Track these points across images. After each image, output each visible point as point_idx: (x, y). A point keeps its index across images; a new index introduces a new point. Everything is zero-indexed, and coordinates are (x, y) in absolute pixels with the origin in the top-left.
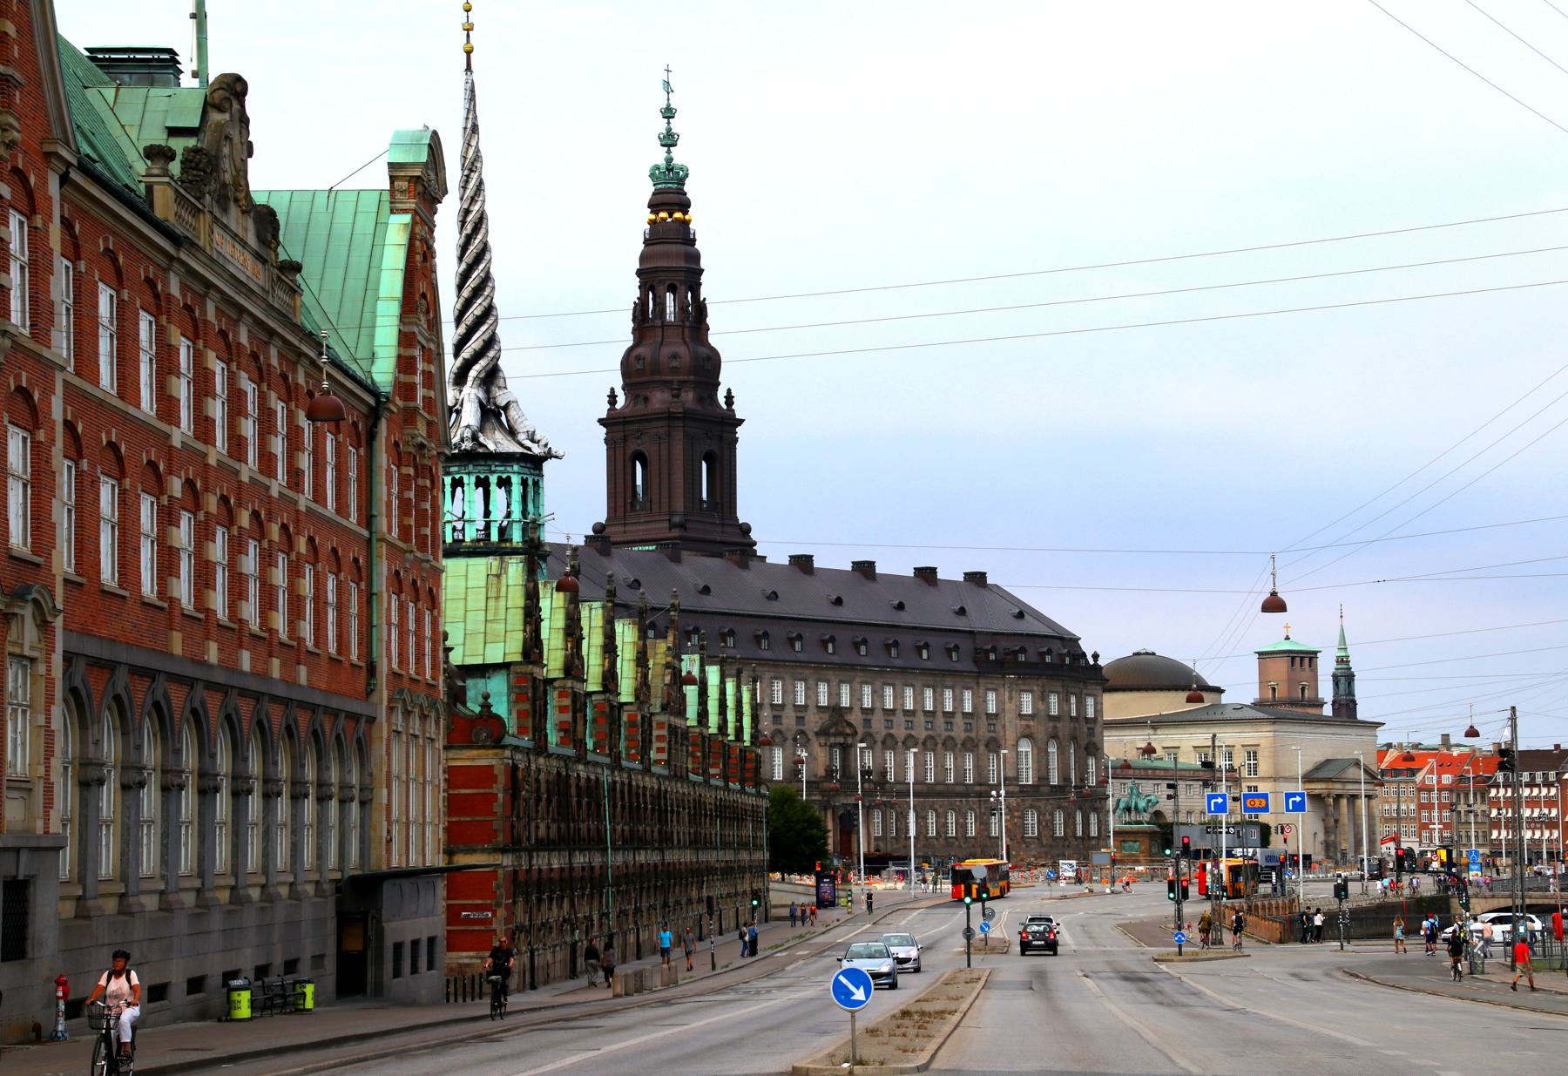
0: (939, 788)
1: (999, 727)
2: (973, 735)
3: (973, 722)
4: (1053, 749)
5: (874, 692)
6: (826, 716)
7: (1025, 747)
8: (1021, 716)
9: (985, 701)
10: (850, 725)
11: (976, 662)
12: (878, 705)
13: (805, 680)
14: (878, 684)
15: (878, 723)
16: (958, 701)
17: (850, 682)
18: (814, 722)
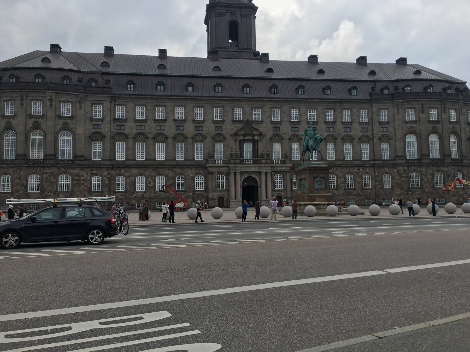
0: (338, 163)
1: (391, 129)
2: (369, 133)
3: (370, 127)
4: (434, 139)
5: (281, 112)
6: (240, 126)
7: (411, 139)
8: (406, 122)
9: (378, 115)
10: (256, 130)
11: (371, 95)
12: (285, 119)
13: (223, 107)
14: (285, 108)
15: (286, 130)
16: (355, 116)
17: (261, 108)
18: (229, 129)
